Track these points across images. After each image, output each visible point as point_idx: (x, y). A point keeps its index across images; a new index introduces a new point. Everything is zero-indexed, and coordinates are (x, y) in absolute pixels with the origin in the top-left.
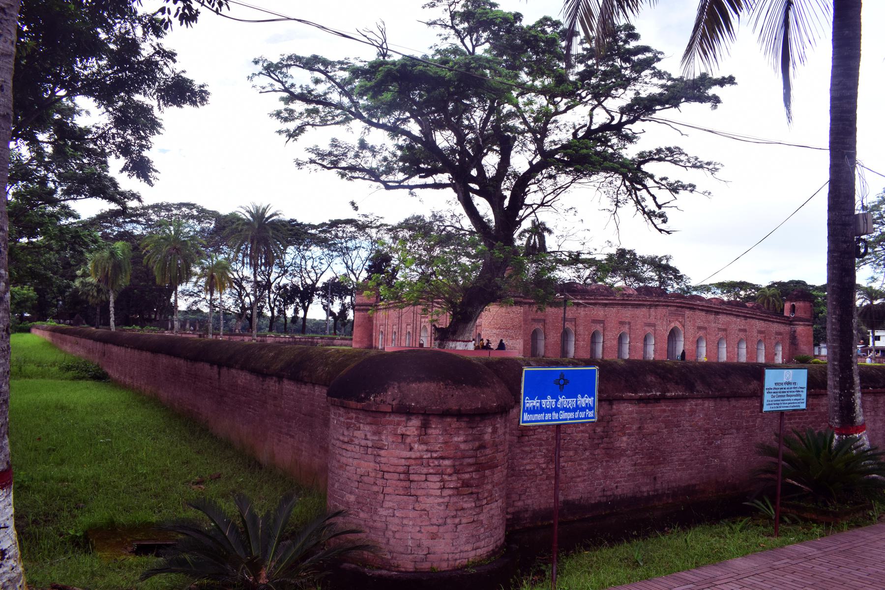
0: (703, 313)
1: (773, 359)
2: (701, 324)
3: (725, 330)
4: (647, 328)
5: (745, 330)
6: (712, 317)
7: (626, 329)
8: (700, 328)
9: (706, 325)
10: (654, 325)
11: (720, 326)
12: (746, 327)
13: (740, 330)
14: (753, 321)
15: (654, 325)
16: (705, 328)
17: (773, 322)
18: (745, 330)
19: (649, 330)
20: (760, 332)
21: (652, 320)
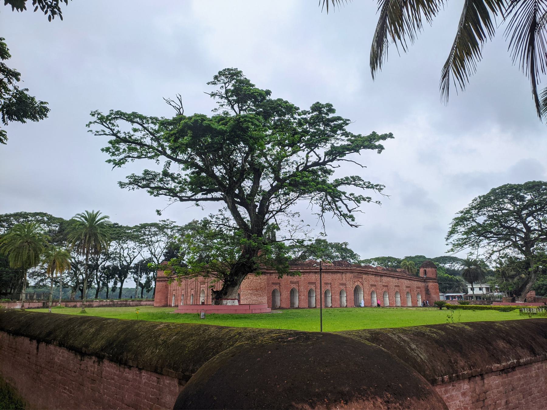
0: (374, 277)
1: (417, 303)
2: (373, 283)
3: (387, 286)
4: (341, 287)
5: (398, 286)
6: (379, 278)
7: (329, 287)
8: (372, 285)
9: (375, 283)
10: (345, 284)
11: (384, 284)
12: (399, 284)
13: (396, 286)
14: (403, 280)
15: (345, 284)
16: (375, 285)
17: (414, 280)
18: (398, 286)
19: (342, 287)
20: (407, 287)
21: (344, 281)
